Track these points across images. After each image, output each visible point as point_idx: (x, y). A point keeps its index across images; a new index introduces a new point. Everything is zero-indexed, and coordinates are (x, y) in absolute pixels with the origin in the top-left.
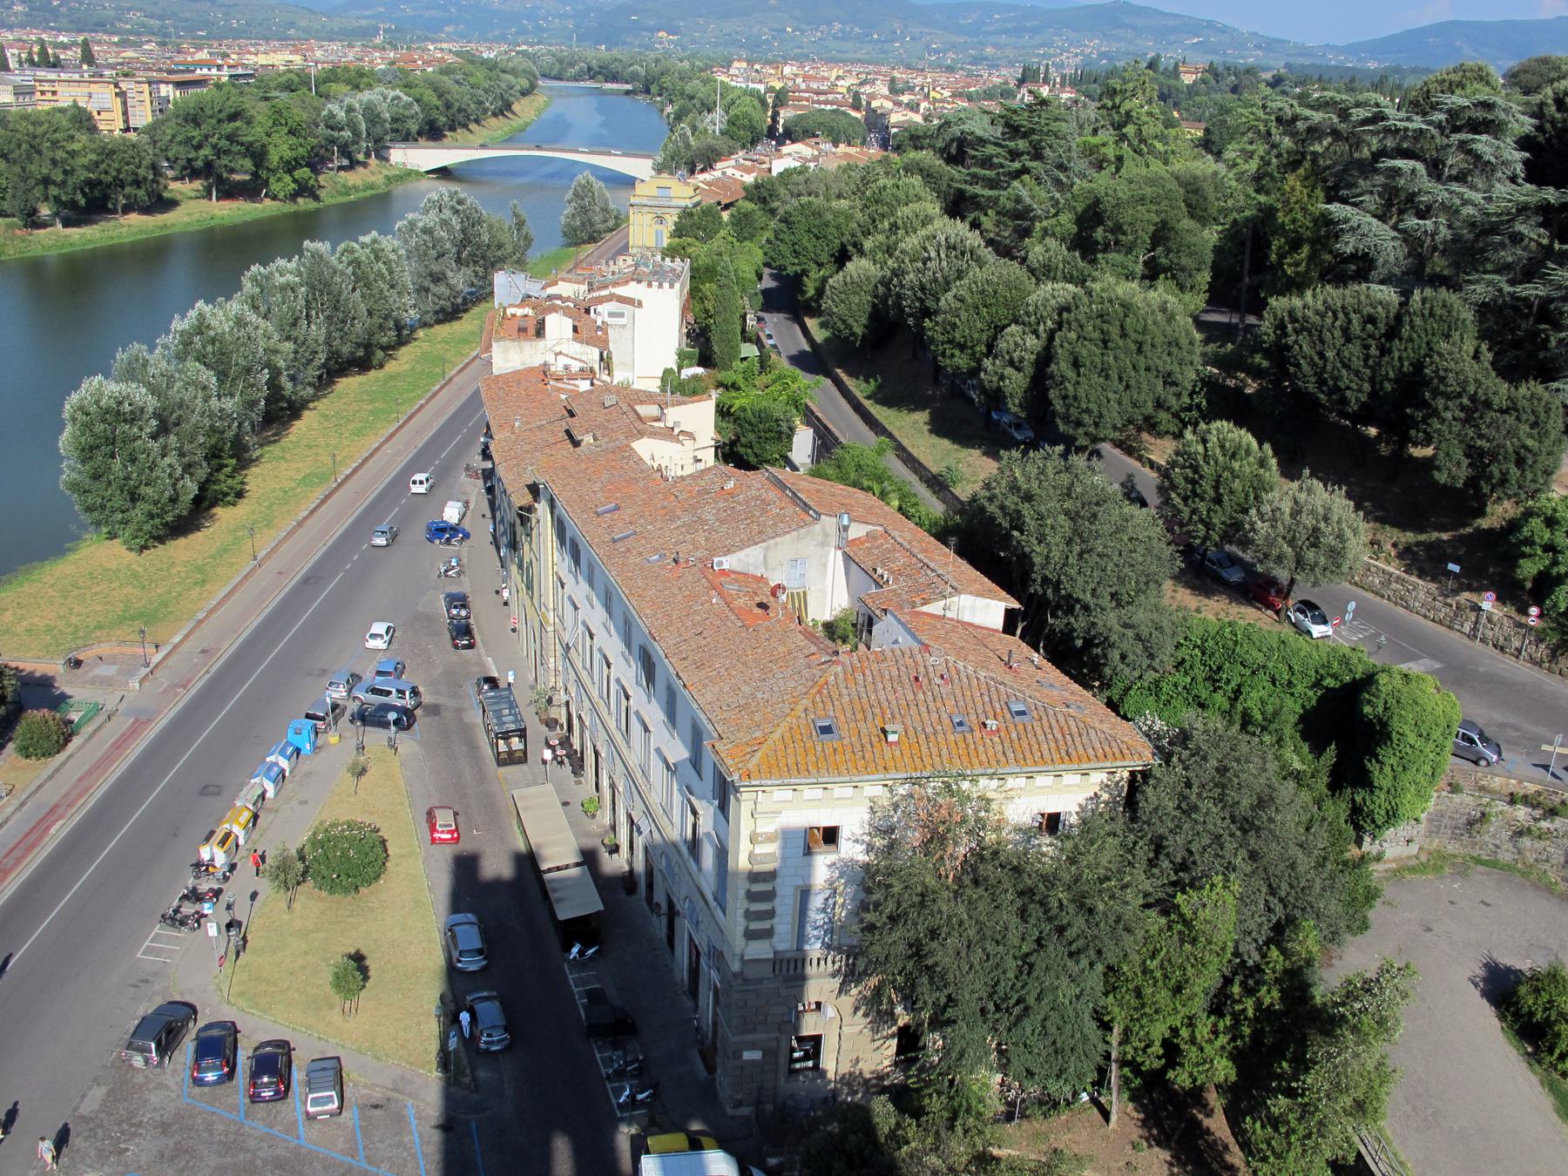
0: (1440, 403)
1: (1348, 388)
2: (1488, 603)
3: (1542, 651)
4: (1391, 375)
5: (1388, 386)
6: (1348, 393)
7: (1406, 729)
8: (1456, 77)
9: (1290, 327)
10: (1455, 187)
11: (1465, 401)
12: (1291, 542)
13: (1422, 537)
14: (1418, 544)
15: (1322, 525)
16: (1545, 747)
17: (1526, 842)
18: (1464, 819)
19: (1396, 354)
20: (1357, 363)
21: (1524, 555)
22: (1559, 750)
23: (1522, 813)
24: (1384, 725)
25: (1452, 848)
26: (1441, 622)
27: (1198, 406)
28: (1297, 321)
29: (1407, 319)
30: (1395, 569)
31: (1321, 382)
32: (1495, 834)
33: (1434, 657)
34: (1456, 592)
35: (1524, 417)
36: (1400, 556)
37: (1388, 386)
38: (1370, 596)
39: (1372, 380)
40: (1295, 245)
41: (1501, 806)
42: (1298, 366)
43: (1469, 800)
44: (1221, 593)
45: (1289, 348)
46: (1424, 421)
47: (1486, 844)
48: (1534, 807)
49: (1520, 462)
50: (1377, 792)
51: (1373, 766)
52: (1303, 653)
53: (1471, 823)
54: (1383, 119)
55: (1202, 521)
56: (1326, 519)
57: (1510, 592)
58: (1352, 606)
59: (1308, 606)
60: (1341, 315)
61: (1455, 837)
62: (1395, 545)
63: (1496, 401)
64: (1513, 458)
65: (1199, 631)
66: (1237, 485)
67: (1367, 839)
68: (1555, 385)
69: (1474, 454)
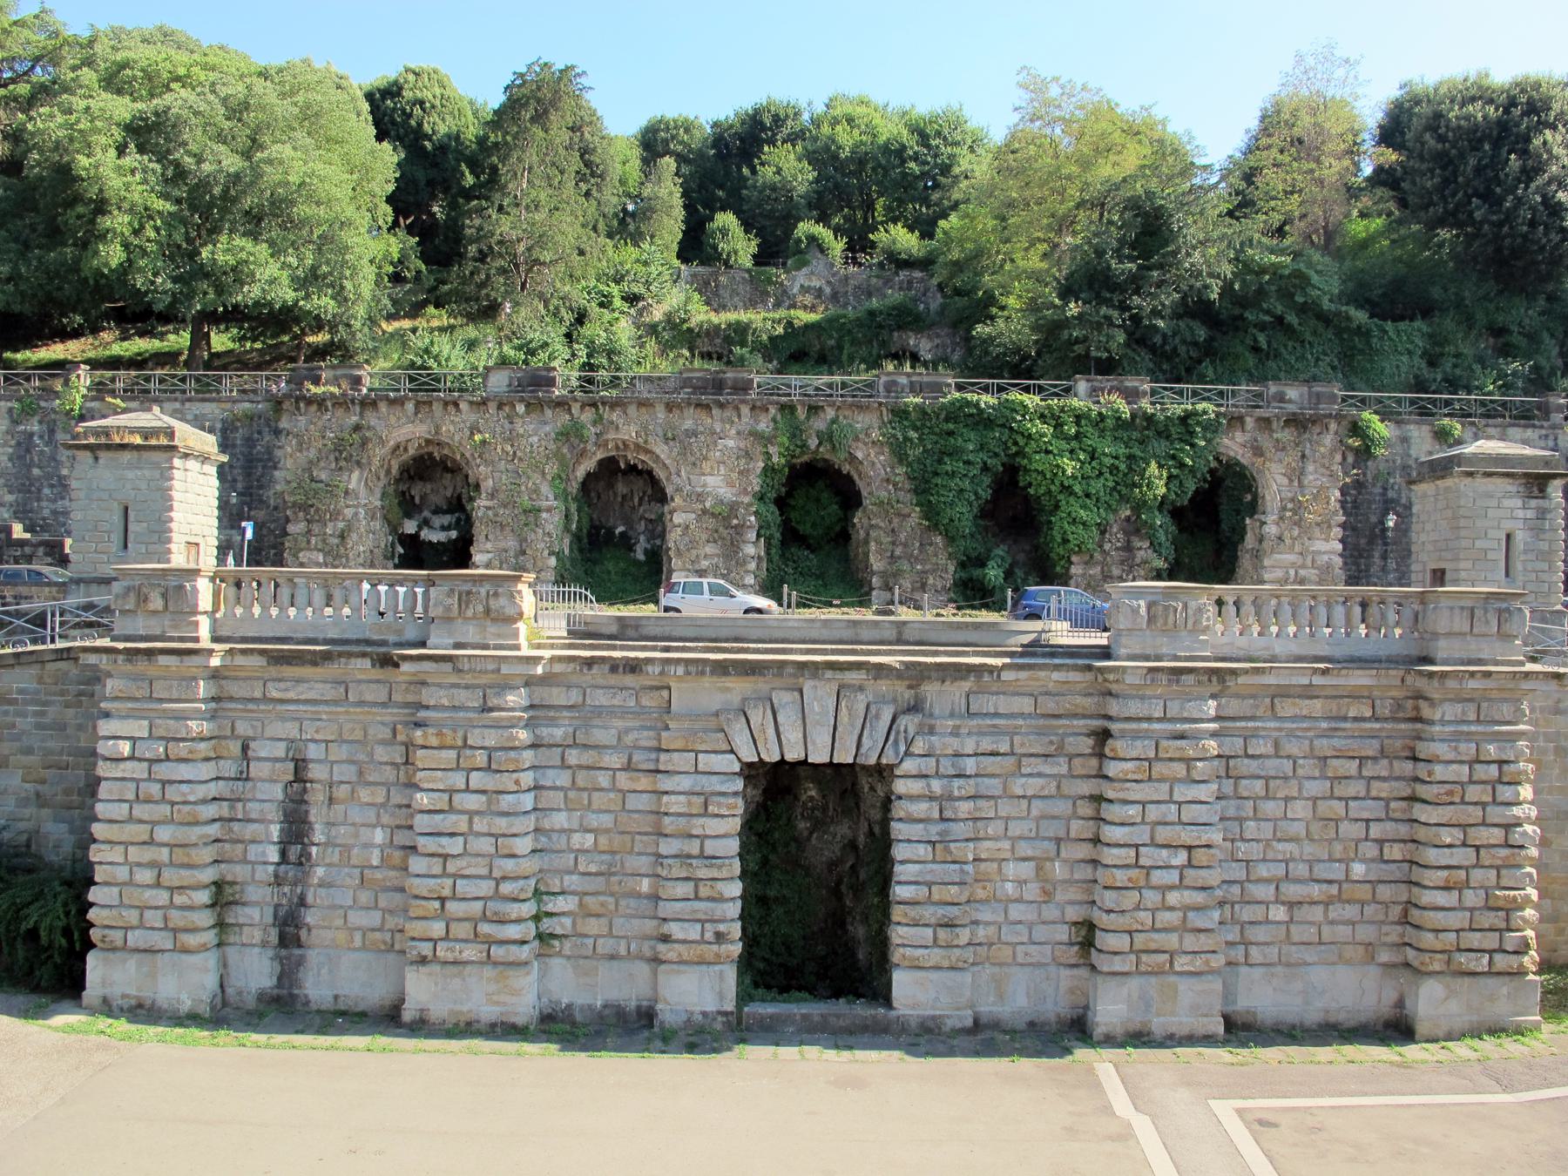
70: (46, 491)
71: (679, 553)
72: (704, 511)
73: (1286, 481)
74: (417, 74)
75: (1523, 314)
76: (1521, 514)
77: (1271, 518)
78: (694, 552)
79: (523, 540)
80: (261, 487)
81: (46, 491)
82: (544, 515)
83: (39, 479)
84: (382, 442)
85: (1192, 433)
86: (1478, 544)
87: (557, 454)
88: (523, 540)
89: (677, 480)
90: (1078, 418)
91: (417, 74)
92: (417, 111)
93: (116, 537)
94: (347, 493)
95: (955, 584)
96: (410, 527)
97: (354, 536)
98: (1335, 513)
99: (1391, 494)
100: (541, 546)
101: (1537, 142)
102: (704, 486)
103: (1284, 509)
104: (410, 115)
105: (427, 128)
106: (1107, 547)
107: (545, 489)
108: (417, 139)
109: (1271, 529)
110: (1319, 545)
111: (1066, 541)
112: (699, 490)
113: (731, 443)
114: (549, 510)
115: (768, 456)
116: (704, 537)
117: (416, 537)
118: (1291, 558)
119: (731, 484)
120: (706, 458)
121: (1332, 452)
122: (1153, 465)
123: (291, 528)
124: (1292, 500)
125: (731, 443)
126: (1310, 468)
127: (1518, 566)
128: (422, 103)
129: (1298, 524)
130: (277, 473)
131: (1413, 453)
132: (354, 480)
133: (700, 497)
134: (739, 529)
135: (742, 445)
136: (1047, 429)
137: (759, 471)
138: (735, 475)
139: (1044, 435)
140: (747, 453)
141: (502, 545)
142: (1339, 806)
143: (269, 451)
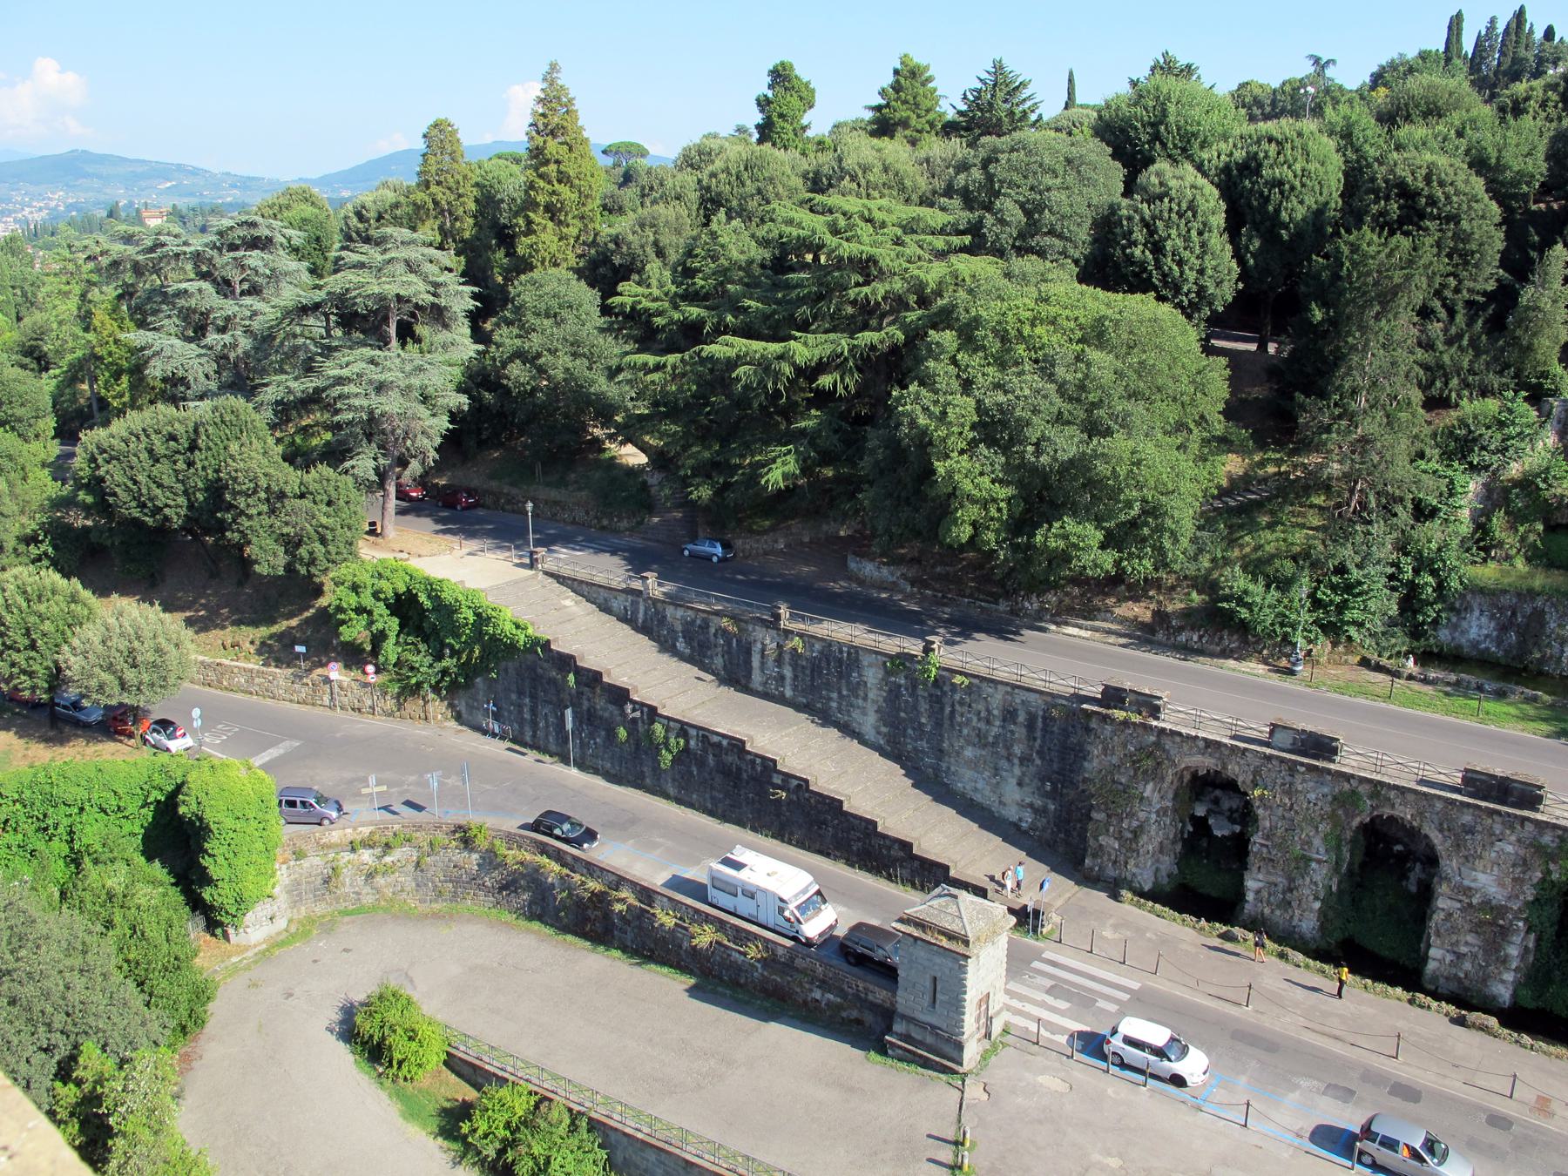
0: (241, 502)
1: (167, 506)
2: (336, 672)
3: (390, 704)
4: (200, 485)
5: (200, 497)
6: (167, 511)
7: (220, 817)
8: (283, 201)
9: (100, 461)
10: (248, 300)
11: (263, 495)
12: (110, 668)
13: (275, 629)
14: (271, 637)
15: (136, 644)
16: (364, 791)
17: (380, 880)
18: (319, 881)
19: (199, 465)
20: (166, 481)
21: (343, 622)
22: (377, 789)
23: (366, 856)
24: (201, 819)
25: (320, 909)
26: (305, 703)
27: (45, 553)
28: (105, 451)
29: (201, 430)
30: (254, 664)
31: (143, 506)
32: (350, 882)
33: (292, 737)
34: (310, 671)
35: (318, 498)
36: (259, 652)
37: (200, 497)
38: (240, 696)
39: (186, 493)
40: (117, 376)
41: (347, 856)
42: (115, 494)
43: (317, 861)
44: (78, 736)
45: (102, 480)
46: (234, 521)
47: (347, 895)
48: (371, 847)
49: (323, 541)
50: (220, 884)
51: (206, 861)
52: (122, 775)
53: (327, 881)
54: (163, 245)
55: (24, 672)
56: (138, 638)
57: (353, 656)
58: (196, 712)
59: (164, 725)
60: (143, 437)
61: (318, 899)
62: (252, 643)
63: (288, 490)
64: (316, 537)
65: (14, 785)
66: (47, 626)
67: (231, 931)
68: (348, 464)
69: (292, 544)
70: (910, 731)
71: (1438, 934)
72: (1470, 905)
74: (1279, 143)
78: (1454, 938)
79: (1291, 880)
80: (1072, 771)
81: (910, 731)
82: (1314, 865)
83: (904, 720)
84: (1174, 764)
87: (1333, 816)
88: (1291, 880)
89: (1450, 865)
91: (1279, 143)
92: (1276, 195)
93: (927, 998)
94: (1142, 798)
96: (1200, 811)
97: (1145, 838)
100: (1307, 892)
102: (1475, 880)
104: (1267, 200)
105: (1284, 216)
107: (1317, 842)
108: (1273, 226)
112: (1466, 883)
113: (1510, 849)
114: (1319, 862)
115: (1549, 872)
116: (1467, 927)
117: (1204, 820)
119: (1502, 885)
120: (1480, 857)
123: (1094, 815)
125: (1510, 849)
128: (1280, 183)
130: (1086, 764)
132: (1149, 790)
133: (1468, 891)
134: (1505, 932)
135: (1522, 852)
137: (1535, 881)
138: (1508, 881)
140: (1525, 860)
141: (1272, 879)
143: (1081, 744)
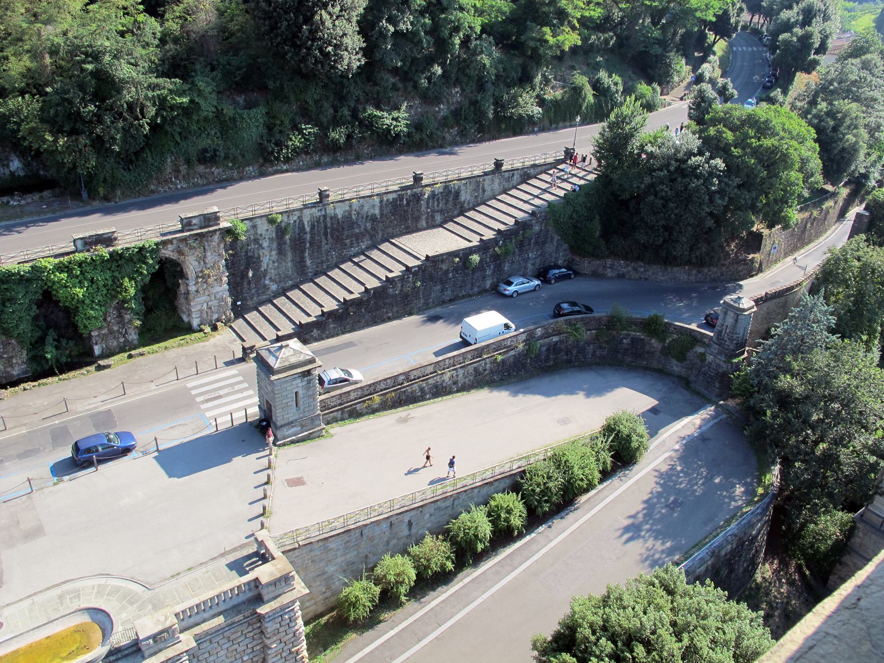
73: (197, 263)
75: (313, 93)
76: (300, 385)
77: (192, 283)
85: (145, 257)
86: (284, 402)
90: (80, 264)
95: (29, 359)
98: (224, 272)
99: (250, 254)
101: (317, 17)
103: (198, 277)
106: (109, 319)
109: (192, 288)
110: (217, 289)
111: (85, 327)
118: (203, 299)
121: (219, 245)
122: (127, 279)
124: (202, 271)
126: (209, 254)
127: (301, 403)
129: (206, 282)
131: (259, 232)
136: (64, 276)
139: (63, 279)
142: (236, 646)
